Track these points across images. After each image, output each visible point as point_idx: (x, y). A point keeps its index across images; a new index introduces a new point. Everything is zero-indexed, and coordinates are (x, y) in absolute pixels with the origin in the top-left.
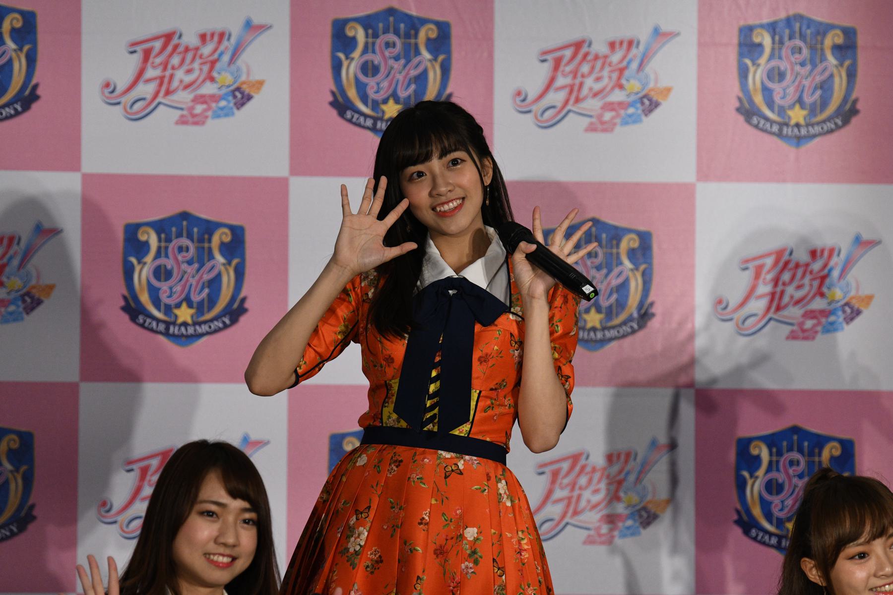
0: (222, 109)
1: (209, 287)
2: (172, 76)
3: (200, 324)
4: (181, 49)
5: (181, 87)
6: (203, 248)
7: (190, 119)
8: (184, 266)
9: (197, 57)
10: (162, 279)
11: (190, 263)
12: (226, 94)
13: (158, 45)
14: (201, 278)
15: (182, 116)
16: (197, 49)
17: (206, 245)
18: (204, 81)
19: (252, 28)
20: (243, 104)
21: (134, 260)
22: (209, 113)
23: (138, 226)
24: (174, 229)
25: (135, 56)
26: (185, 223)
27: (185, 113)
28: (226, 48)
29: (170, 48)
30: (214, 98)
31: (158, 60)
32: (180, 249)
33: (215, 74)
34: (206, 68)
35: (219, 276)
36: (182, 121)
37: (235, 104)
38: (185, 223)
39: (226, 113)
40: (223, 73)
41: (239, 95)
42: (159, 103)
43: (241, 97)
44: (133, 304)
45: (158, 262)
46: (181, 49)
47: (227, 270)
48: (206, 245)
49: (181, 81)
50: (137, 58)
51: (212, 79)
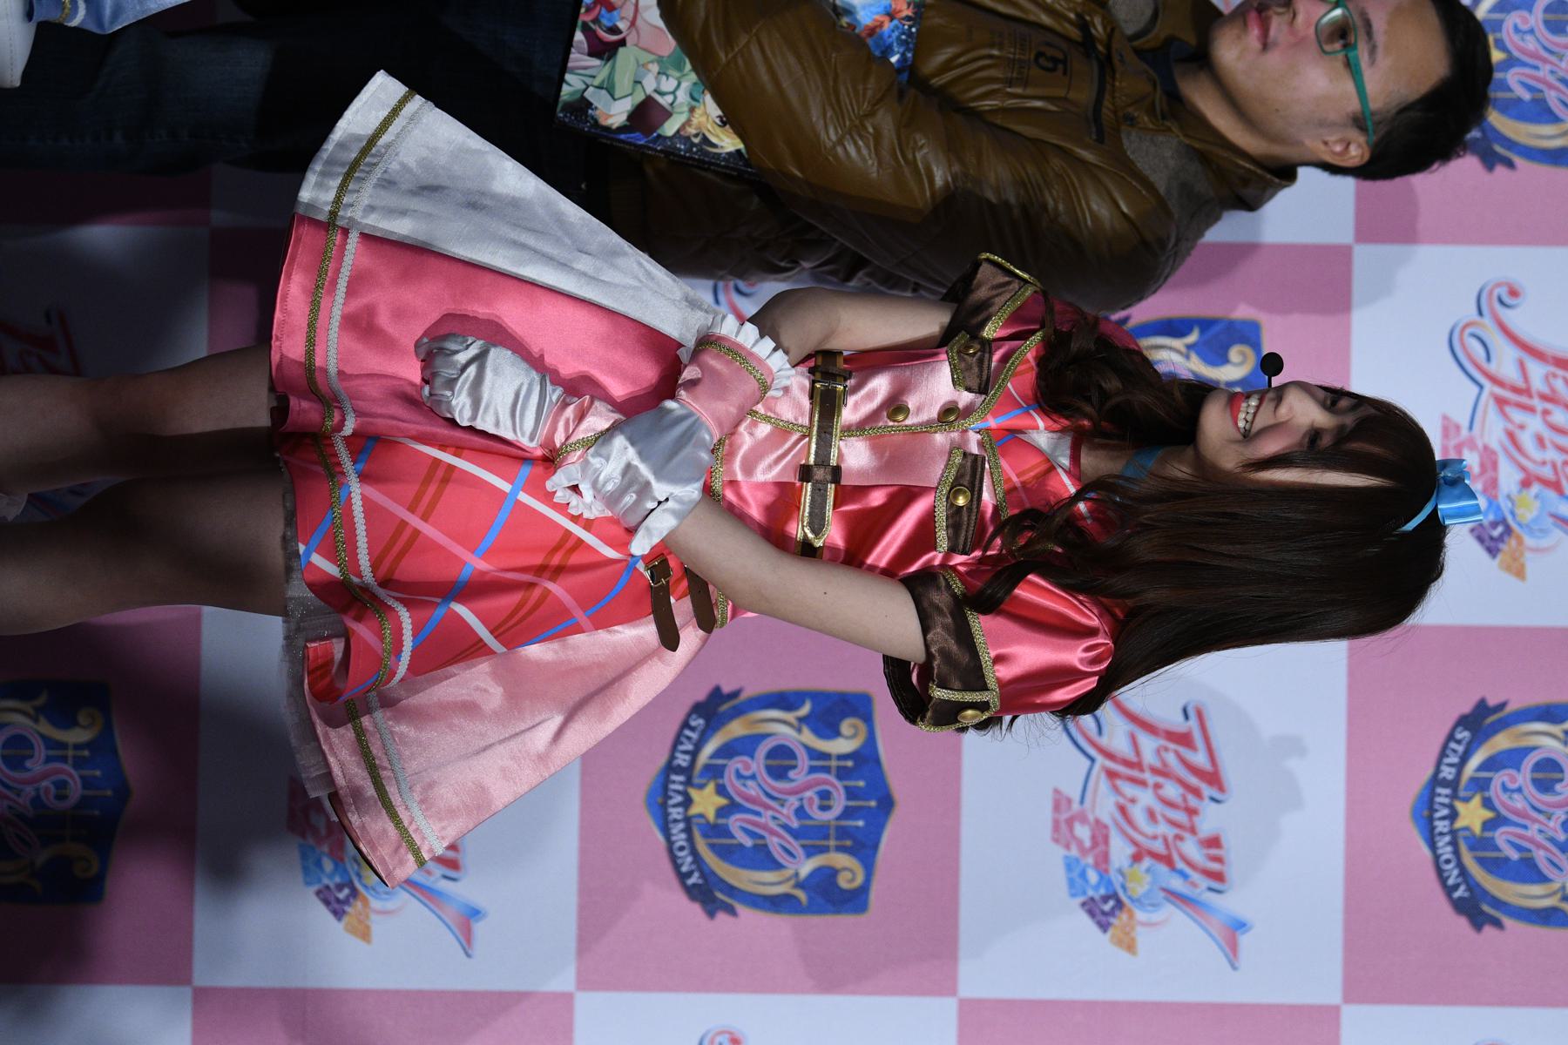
0: (1083, 875)
1: (755, 846)
2: (1143, 783)
3: (688, 830)
4: (1193, 801)
5: (1121, 801)
6: (827, 837)
7: (1064, 816)
8: (793, 802)
9: (1176, 831)
10: (771, 762)
11: (800, 812)
12: (1110, 882)
13: (1200, 758)
14: (773, 833)
15: (1069, 801)
16: (1193, 831)
17: (832, 843)
18: (1134, 843)
19: (1232, 933)
20: (1091, 913)
21: (805, 710)
22: (1074, 852)
23: (868, 718)
24: (861, 784)
25: (1181, 718)
26: (873, 804)
27: (1076, 806)
28: (1194, 885)
29: (1193, 781)
30: (1103, 861)
31: (1171, 759)
32: (825, 795)
33: (1147, 862)
34: (1158, 846)
35: (777, 866)
36: (1060, 802)
37: (1092, 899)
38: (873, 804)
39: (1076, 881)
40: (1148, 878)
41: (1107, 907)
42: (1092, 760)
43: (1105, 909)
44: (724, 707)
45: (802, 755)
46: (1193, 801)
47: (788, 880)
48: (832, 843)
49: (1133, 801)
50: (1176, 722)
51: (1137, 858)
